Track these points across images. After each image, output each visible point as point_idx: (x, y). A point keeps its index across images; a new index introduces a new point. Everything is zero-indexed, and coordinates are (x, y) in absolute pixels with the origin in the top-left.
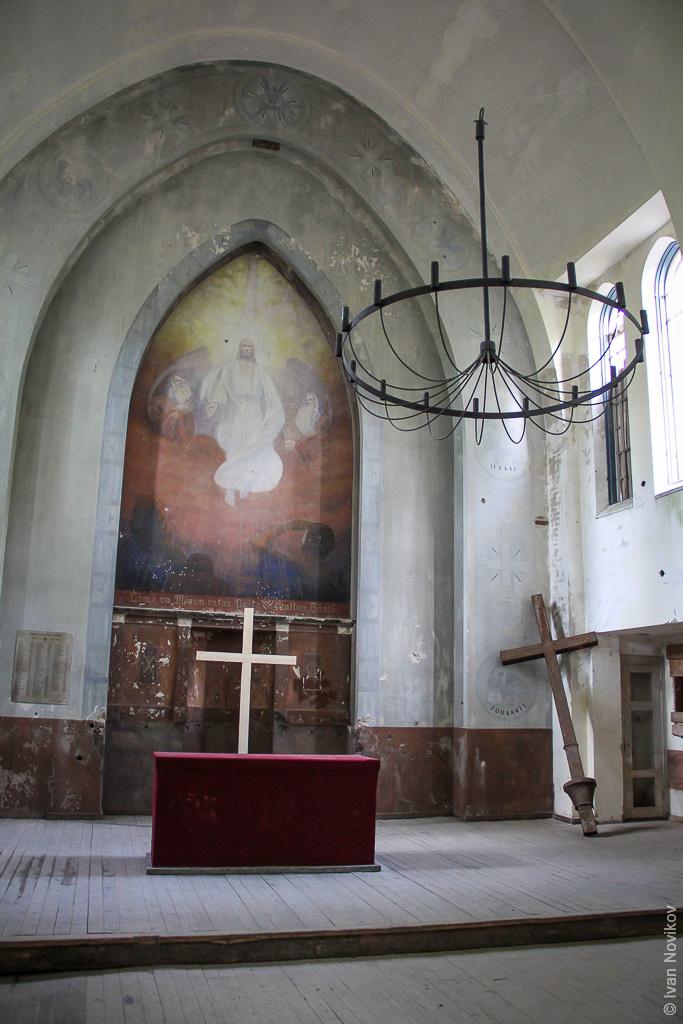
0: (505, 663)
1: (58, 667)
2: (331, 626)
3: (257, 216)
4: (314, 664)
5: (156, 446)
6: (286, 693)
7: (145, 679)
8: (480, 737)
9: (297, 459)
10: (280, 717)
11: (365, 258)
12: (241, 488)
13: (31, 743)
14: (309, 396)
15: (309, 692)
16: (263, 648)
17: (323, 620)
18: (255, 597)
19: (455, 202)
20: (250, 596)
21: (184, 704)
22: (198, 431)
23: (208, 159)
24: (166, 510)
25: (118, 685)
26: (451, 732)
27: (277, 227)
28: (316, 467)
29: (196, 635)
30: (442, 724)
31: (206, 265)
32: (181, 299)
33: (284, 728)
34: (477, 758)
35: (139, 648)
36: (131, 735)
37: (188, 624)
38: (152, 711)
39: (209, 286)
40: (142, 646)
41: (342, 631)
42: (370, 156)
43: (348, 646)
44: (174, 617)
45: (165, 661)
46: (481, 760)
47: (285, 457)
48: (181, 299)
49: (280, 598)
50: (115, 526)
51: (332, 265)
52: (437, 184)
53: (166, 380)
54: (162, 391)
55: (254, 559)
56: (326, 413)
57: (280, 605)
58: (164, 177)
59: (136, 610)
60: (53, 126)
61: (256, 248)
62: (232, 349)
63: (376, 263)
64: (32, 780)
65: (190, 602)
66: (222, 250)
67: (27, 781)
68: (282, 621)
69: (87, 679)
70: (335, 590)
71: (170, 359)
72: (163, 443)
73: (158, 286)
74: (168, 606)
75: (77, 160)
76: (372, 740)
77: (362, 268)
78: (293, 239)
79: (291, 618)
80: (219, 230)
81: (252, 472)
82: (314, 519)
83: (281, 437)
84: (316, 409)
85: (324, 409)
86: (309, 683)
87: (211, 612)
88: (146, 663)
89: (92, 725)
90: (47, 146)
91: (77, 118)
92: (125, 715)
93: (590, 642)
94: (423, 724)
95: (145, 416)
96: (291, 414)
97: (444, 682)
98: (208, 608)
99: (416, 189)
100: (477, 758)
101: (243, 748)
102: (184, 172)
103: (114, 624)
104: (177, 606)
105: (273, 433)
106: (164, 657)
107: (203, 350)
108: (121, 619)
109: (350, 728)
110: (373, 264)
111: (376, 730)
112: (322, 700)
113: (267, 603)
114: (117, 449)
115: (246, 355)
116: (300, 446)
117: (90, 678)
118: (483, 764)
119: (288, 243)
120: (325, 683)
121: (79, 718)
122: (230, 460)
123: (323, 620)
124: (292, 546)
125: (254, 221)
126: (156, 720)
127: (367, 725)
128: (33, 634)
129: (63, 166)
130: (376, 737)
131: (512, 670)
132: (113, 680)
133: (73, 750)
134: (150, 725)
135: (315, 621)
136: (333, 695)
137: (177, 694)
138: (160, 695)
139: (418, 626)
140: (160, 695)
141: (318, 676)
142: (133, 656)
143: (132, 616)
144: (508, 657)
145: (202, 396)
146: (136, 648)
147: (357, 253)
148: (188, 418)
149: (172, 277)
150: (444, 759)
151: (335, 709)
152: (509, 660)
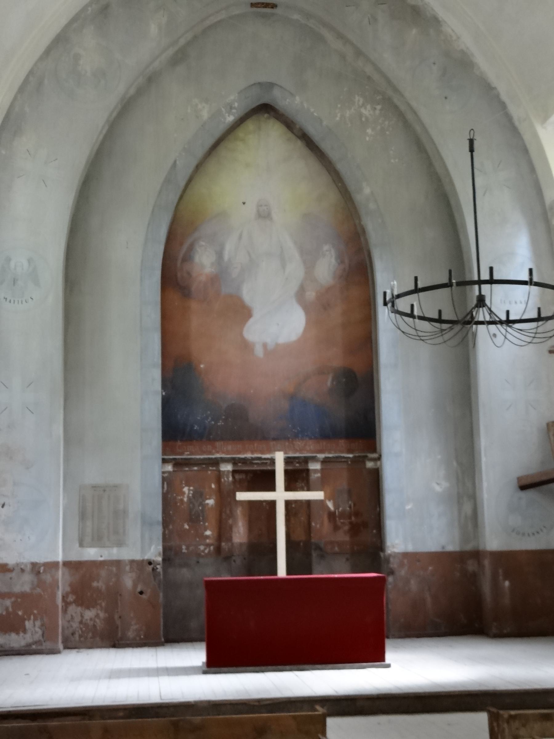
0: (523, 487)
1: (120, 515)
2: (360, 461)
3: (263, 79)
4: (345, 496)
6: (322, 524)
7: (195, 518)
8: (506, 560)
9: (318, 309)
10: (318, 548)
11: (369, 107)
12: (269, 341)
13: (98, 582)
14: (326, 247)
15: (342, 523)
16: (299, 484)
17: (351, 456)
18: (286, 438)
19: (454, 38)
20: (280, 438)
21: (230, 539)
23: (210, 27)
24: (202, 366)
25: (171, 527)
26: (477, 555)
27: (281, 87)
29: (237, 477)
30: (469, 547)
31: (217, 134)
33: (322, 557)
34: (501, 578)
35: (187, 492)
36: (184, 571)
37: (227, 468)
38: (202, 548)
39: (222, 151)
40: (189, 490)
41: (370, 465)
43: (376, 477)
44: (216, 463)
45: (211, 502)
46: (505, 579)
47: (306, 307)
48: (198, 167)
49: (311, 439)
50: (157, 386)
51: (338, 119)
52: (436, 21)
53: (191, 248)
54: (188, 258)
56: (342, 262)
57: (311, 445)
58: (171, 52)
59: (182, 459)
60: (64, 21)
63: (381, 110)
64: (102, 615)
65: (230, 448)
66: (230, 119)
67: (97, 616)
68: (314, 459)
69: (144, 523)
70: (360, 428)
72: (194, 305)
73: (175, 162)
74: (210, 453)
75: (89, 50)
76: (402, 565)
77: (367, 119)
78: (298, 98)
79: (321, 456)
81: (276, 324)
84: (333, 261)
85: (340, 259)
86: (342, 515)
87: (249, 455)
88: (194, 505)
89: (150, 563)
90: (61, 40)
91: (84, 9)
92: (178, 552)
94: (450, 548)
95: (174, 280)
96: (309, 267)
97: (468, 508)
98: (245, 451)
99: (414, 31)
100: (501, 578)
101: (282, 572)
102: (189, 44)
103: (163, 473)
104: (218, 452)
105: (294, 287)
106: (210, 499)
108: (169, 468)
109: (382, 554)
110: (377, 112)
111: (405, 555)
112: (355, 530)
113: (299, 443)
114: (153, 316)
115: (264, 214)
117: (146, 522)
118: (507, 583)
119: (292, 102)
120: (357, 514)
121: (138, 557)
123: (351, 456)
124: (320, 389)
125: (259, 83)
126: (207, 555)
127: (396, 550)
128: (94, 487)
129: (77, 57)
130: (405, 561)
131: (530, 494)
132: (165, 523)
133: (135, 585)
134: (201, 560)
135: (344, 457)
136: (365, 525)
138: (208, 533)
139: (439, 457)
140: (208, 533)
141: (350, 507)
142: (182, 500)
143: (178, 464)
144: (524, 482)
145: (226, 257)
146: (184, 493)
147: (361, 102)
148: (215, 280)
150: (473, 579)
152: (525, 486)
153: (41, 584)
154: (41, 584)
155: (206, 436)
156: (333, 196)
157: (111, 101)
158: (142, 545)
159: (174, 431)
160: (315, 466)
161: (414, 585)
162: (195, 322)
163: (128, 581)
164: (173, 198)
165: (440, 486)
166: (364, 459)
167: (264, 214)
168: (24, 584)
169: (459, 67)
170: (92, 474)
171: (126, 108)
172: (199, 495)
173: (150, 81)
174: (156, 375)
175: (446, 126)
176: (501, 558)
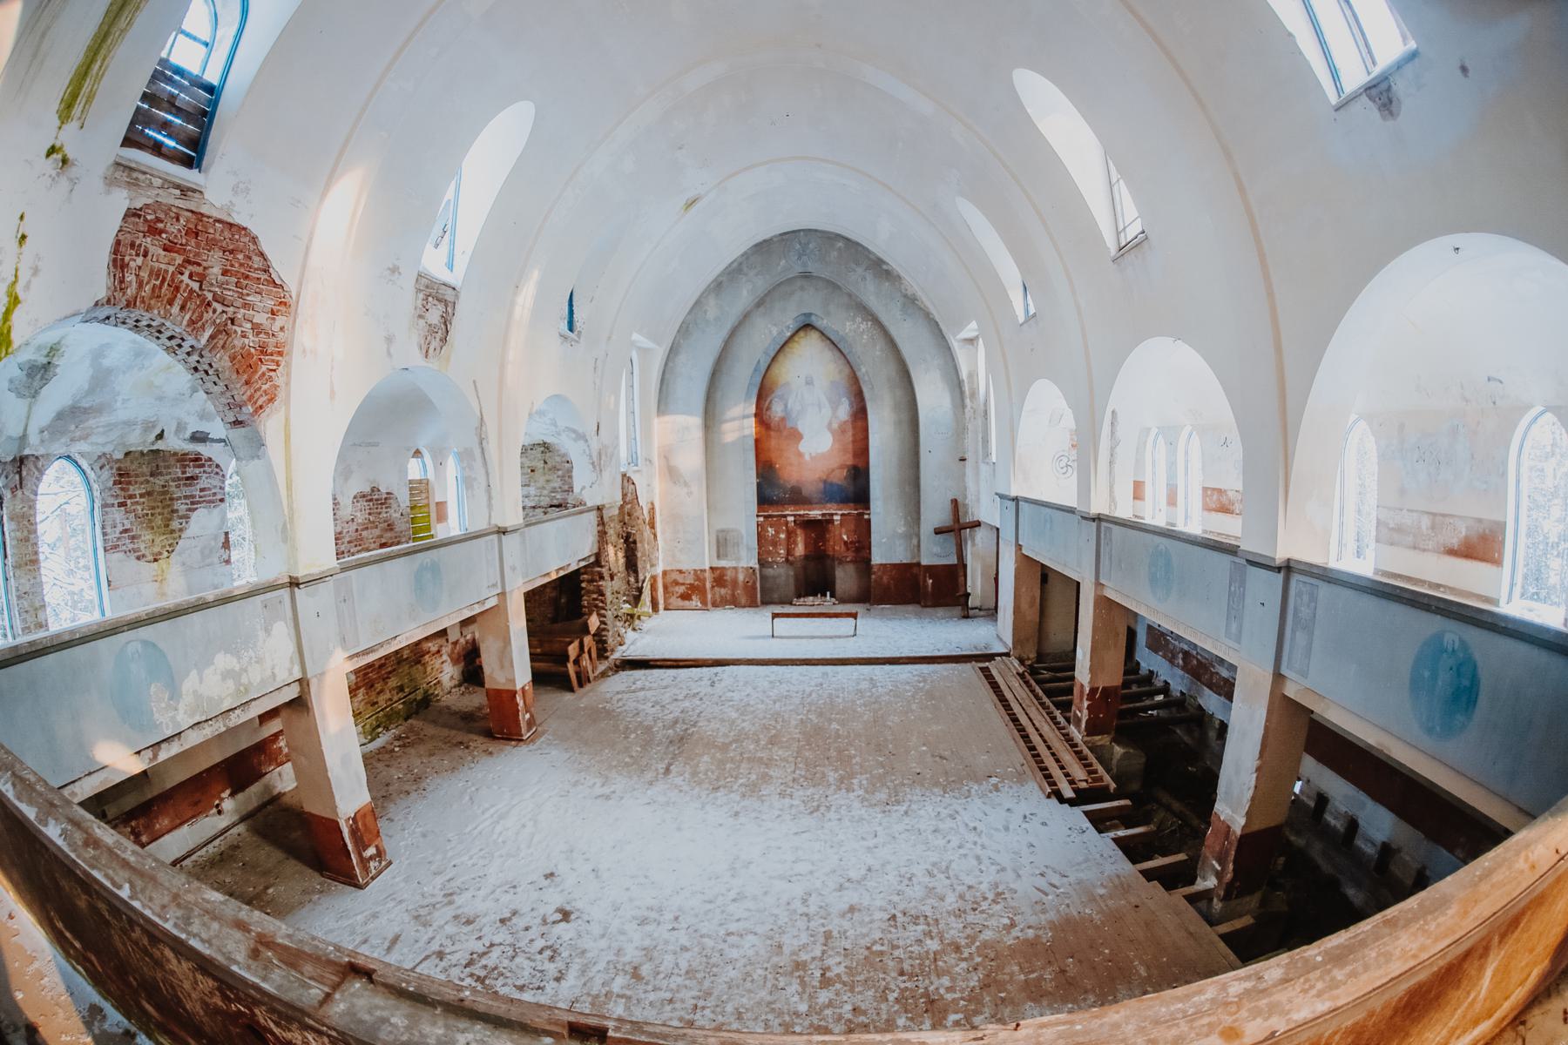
5: (769, 436)
7: (775, 544)
8: (931, 570)
22: (789, 425)
26: (918, 564)
28: (849, 436)
37: (791, 519)
39: (786, 349)
42: (860, 270)
45: (783, 536)
50: (754, 480)
52: (899, 277)
55: (821, 485)
61: (807, 326)
80: (789, 323)
82: (850, 463)
83: (830, 424)
85: (851, 405)
90: (698, 303)
93: (978, 524)
97: (915, 541)
105: (826, 422)
107: (787, 384)
112: (857, 550)
115: (809, 382)
116: (840, 426)
117: (749, 549)
119: (821, 323)
124: (839, 477)
132: (760, 547)
148: (783, 419)
151: (863, 554)
153: (698, 579)
154: (698, 579)
155: (780, 503)
156: (847, 370)
157: (724, 333)
158: (745, 558)
159: (764, 500)
161: (885, 579)
162: (773, 443)
163: (741, 577)
164: (759, 379)
165: (901, 530)
167: (809, 382)
169: (911, 302)
170: (723, 523)
171: (734, 332)
172: (777, 532)
173: (746, 316)
175: (908, 334)
176: (929, 568)
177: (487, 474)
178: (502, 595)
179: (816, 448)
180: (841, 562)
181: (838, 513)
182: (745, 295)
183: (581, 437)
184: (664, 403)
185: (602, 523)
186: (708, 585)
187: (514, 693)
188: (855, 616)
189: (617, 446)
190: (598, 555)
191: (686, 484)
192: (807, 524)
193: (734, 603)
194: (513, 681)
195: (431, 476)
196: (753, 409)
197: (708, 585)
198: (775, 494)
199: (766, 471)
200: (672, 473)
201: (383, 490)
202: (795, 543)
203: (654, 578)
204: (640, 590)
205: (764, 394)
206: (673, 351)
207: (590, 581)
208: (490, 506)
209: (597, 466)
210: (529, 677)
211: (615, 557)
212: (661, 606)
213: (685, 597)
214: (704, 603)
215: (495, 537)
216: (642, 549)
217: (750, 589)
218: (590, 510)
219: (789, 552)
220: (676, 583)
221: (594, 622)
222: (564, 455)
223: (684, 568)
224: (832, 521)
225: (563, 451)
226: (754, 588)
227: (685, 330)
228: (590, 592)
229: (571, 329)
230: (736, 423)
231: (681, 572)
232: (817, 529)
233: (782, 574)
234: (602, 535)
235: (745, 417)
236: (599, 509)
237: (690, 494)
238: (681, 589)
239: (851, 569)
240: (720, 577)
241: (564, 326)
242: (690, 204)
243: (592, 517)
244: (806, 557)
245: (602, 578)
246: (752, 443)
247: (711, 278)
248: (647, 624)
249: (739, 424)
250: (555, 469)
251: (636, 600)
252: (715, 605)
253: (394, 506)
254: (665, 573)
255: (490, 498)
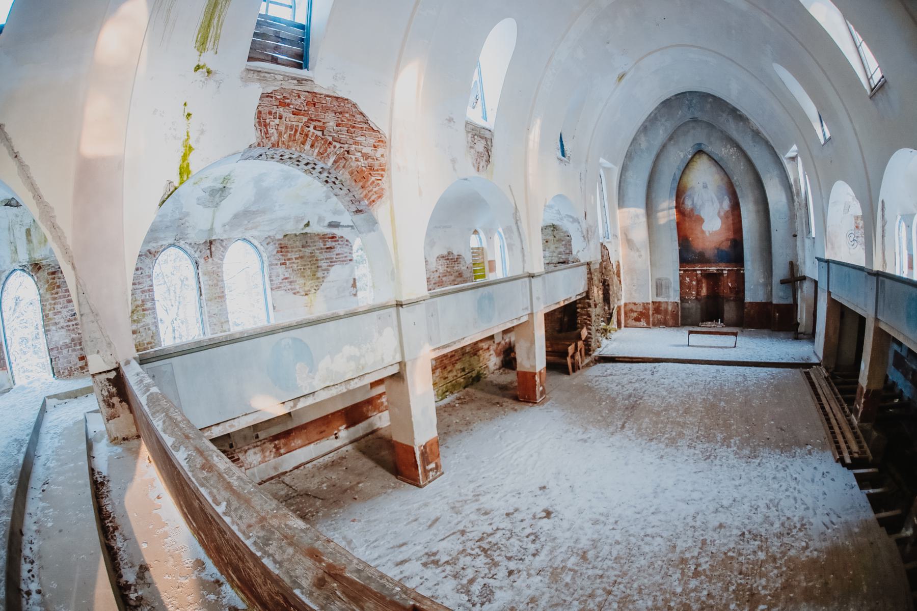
7: (689, 288)
22: (696, 213)
32: (683, 172)
37: (699, 272)
48: (683, 172)
50: (677, 248)
54: (683, 203)
55: (716, 251)
62: (701, 184)
71: (684, 192)
75: (643, 142)
83: (719, 213)
90: (634, 139)
107: (692, 188)
115: (705, 187)
117: (675, 291)
122: (706, 221)
124: (726, 246)
137: (698, 293)
148: (692, 210)
149: (678, 169)
153: (645, 308)
157: (653, 157)
159: (683, 261)
160: (725, 272)
163: (670, 308)
164: (676, 185)
166: (739, 270)
167: (705, 187)
168: (640, 309)
170: (659, 275)
171: (658, 157)
172: (691, 281)
173: (664, 147)
174: (676, 244)
177: (521, 242)
178: (531, 315)
179: (712, 227)
180: (728, 300)
181: (726, 269)
182: (661, 134)
183: (575, 220)
184: (622, 201)
185: (590, 273)
186: (651, 312)
187: (535, 374)
188: (735, 334)
189: (597, 226)
190: (588, 292)
191: (638, 250)
192: (708, 276)
193: (665, 324)
194: (534, 367)
195: (485, 245)
196: (674, 204)
197: (651, 312)
198: (691, 256)
199: (685, 243)
200: (629, 242)
201: (455, 253)
202: (701, 287)
203: (619, 307)
204: (611, 314)
205: (680, 193)
206: (624, 169)
207: (582, 308)
208: (524, 261)
209: (586, 238)
210: (544, 365)
211: (597, 294)
212: (623, 325)
213: (637, 319)
214: (648, 323)
215: (527, 279)
216: (613, 289)
217: (675, 315)
218: (583, 265)
219: (698, 293)
220: (632, 311)
221: (584, 333)
222: (566, 232)
223: (637, 302)
224: (723, 274)
225: (565, 230)
226: (677, 315)
227: (629, 156)
228: (582, 315)
229: (563, 154)
230: (665, 212)
231: (635, 304)
232: (713, 279)
233: (693, 306)
234: (590, 280)
235: (670, 208)
236: (588, 264)
237: (640, 256)
238: (635, 315)
239: (732, 304)
240: (657, 307)
241: (559, 154)
242: (621, 77)
243: (584, 269)
244: (708, 296)
245: (590, 306)
246: (675, 224)
247: (640, 124)
248: (614, 335)
249: (667, 214)
250: (560, 240)
251: (609, 321)
252: (654, 325)
253: (462, 262)
254: (625, 305)
255: (523, 256)
